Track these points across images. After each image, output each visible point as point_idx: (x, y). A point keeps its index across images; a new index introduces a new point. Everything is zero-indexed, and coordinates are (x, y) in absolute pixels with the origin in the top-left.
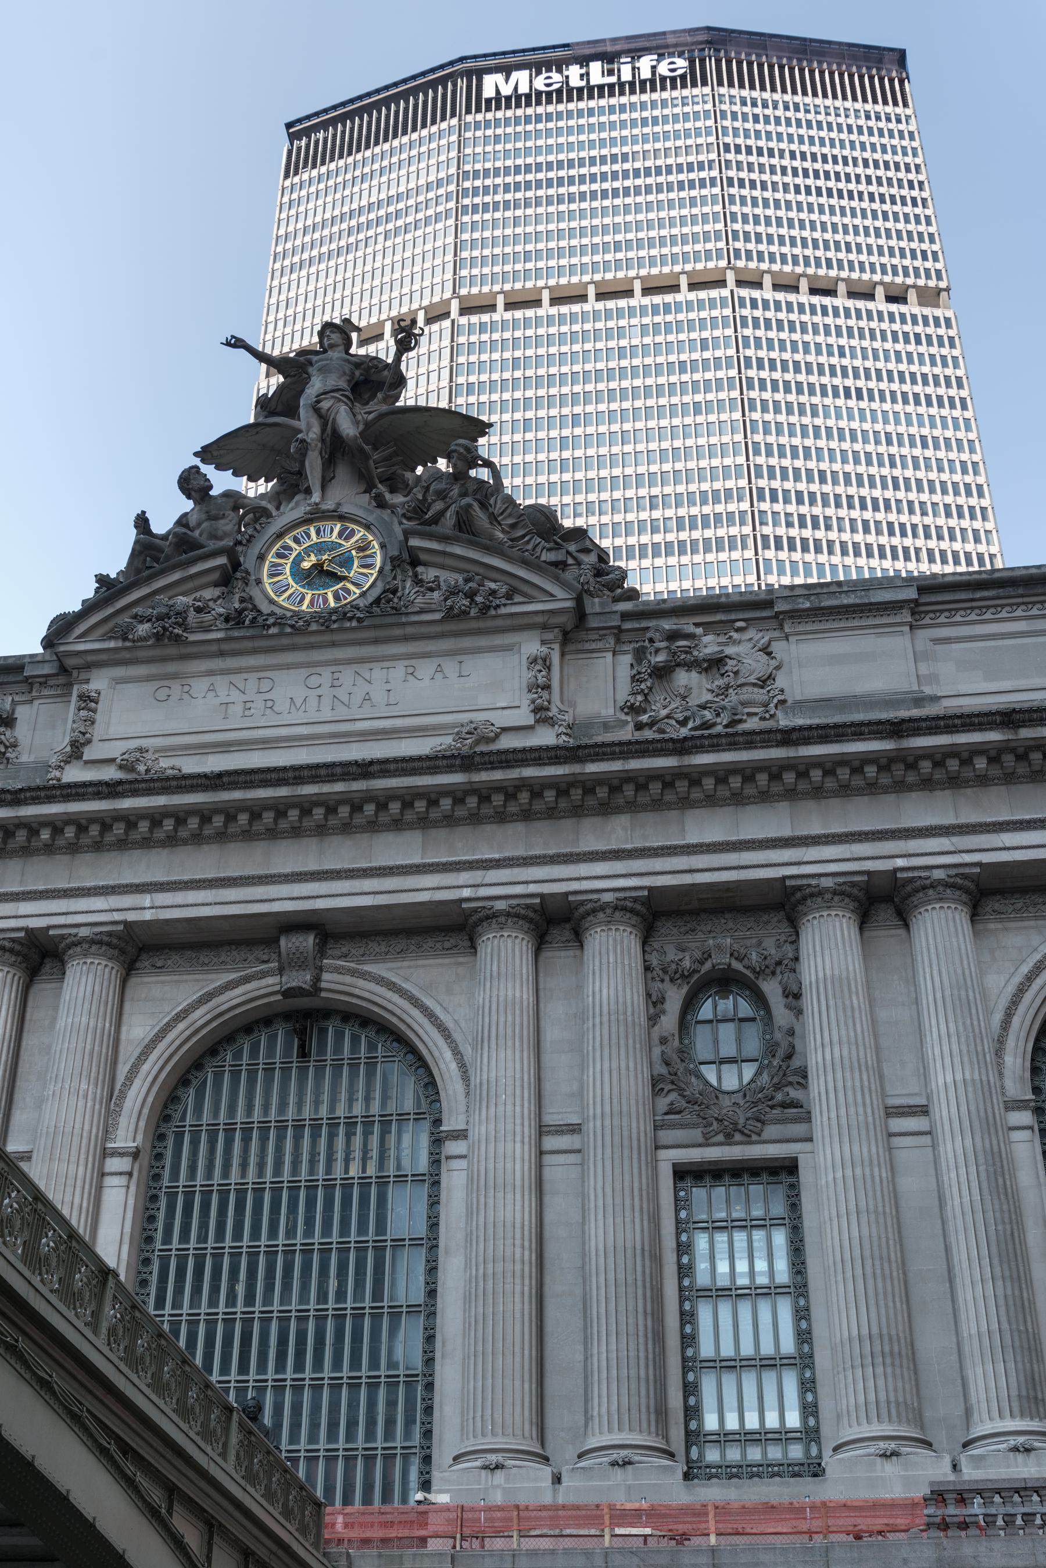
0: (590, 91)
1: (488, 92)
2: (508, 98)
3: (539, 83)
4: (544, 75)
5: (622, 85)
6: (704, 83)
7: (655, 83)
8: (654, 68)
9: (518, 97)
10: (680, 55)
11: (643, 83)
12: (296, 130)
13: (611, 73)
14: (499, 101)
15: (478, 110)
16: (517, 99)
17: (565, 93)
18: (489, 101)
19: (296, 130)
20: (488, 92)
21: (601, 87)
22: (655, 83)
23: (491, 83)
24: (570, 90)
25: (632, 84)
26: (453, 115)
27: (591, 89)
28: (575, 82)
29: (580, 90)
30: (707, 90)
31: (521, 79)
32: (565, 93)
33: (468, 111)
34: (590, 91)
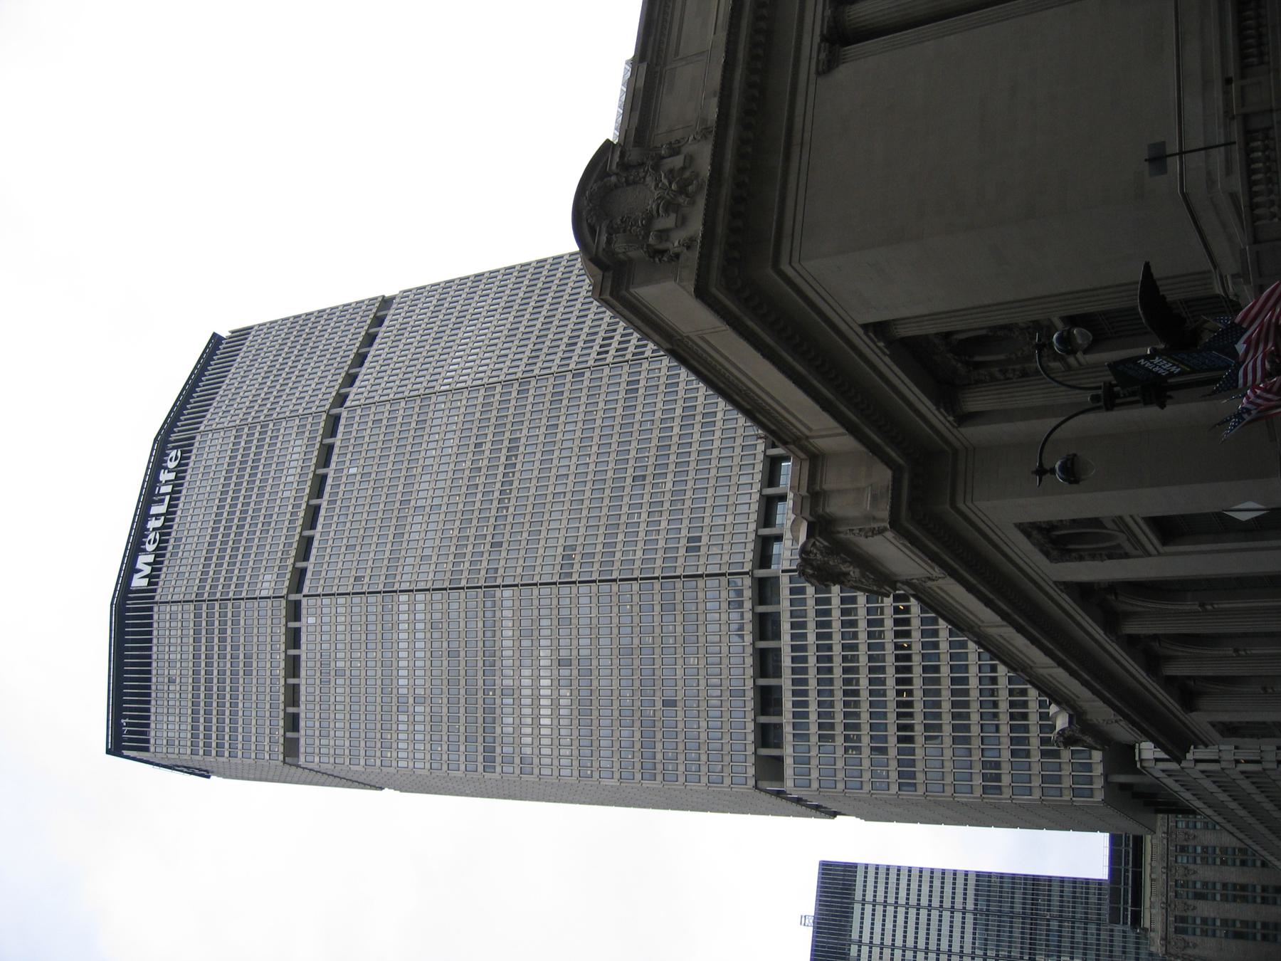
0: (169, 516)
2: (153, 570)
3: (150, 547)
5: (173, 492)
6: (194, 438)
7: (180, 472)
9: (155, 562)
11: (177, 478)
12: (116, 748)
13: (162, 501)
14: (153, 578)
16: (156, 566)
17: (164, 531)
19: (116, 748)
20: (145, 582)
21: (169, 506)
22: (180, 472)
23: (138, 582)
24: (163, 527)
27: (168, 513)
28: (159, 523)
30: (198, 438)
31: (143, 561)
32: (164, 531)
33: (153, 597)
34: (169, 516)
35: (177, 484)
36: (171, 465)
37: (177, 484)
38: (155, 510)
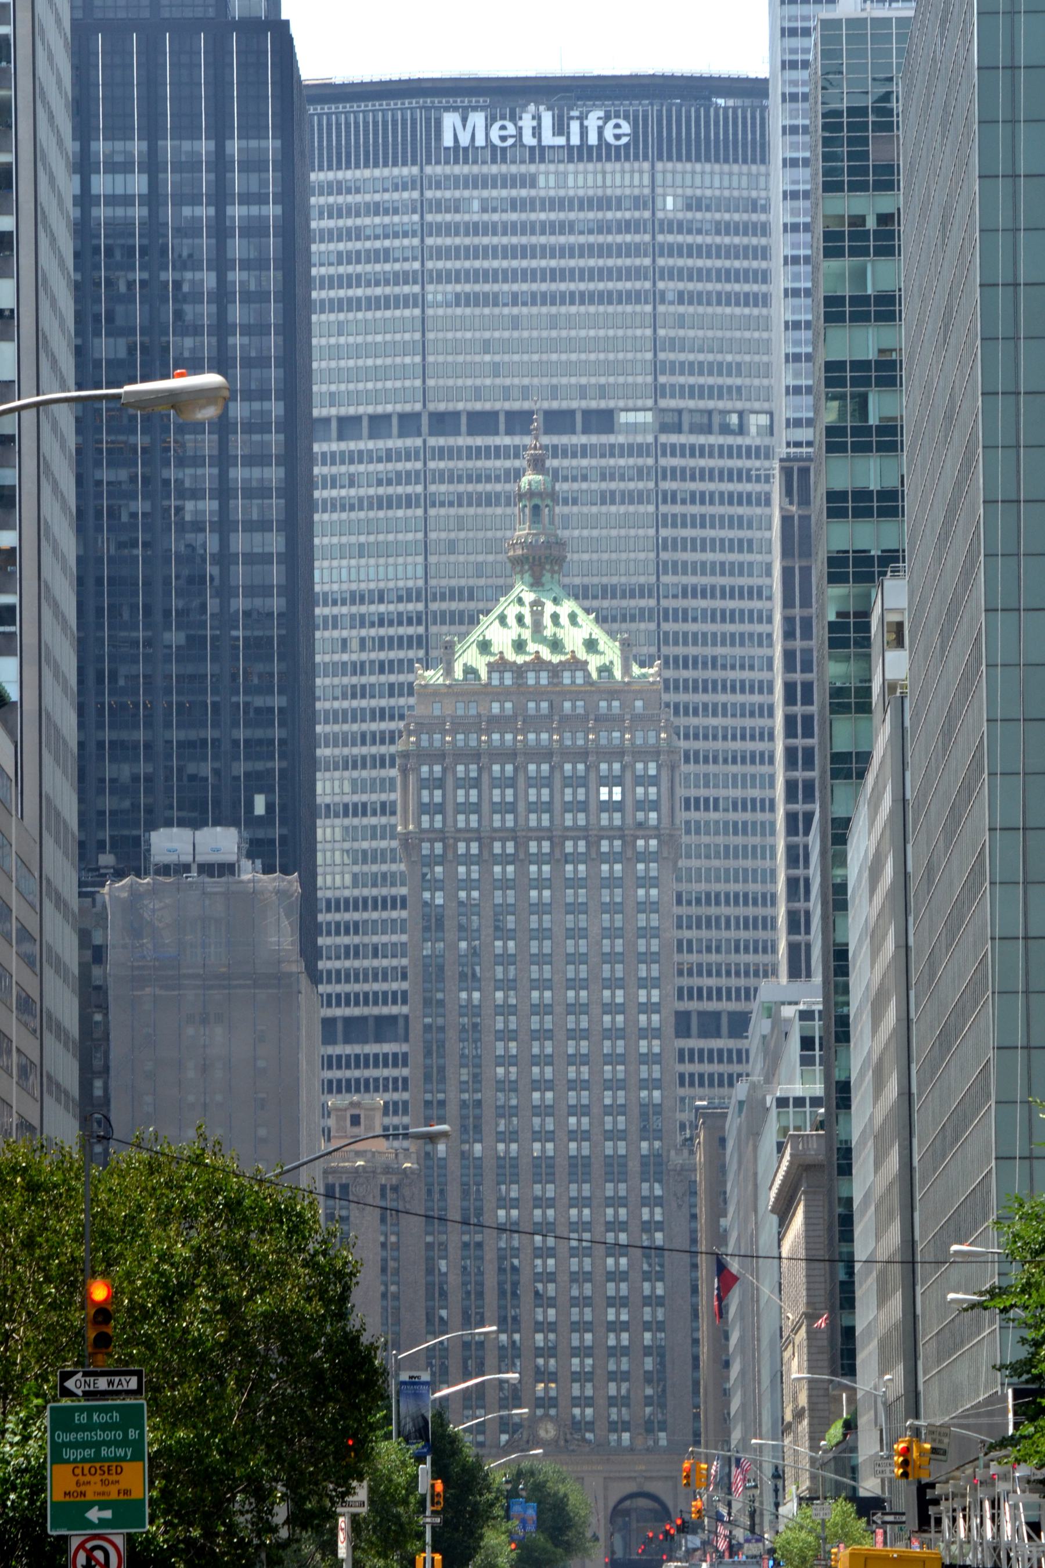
0: (539, 153)
1: (448, 141)
2: (466, 149)
4: (499, 124)
5: (570, 148)
6: (646, 158)
8: (600, 130)
10: (626, 118)
11: (590, 148)
14: (460, 153)
15: (438, 163)
18: (447, 149)
23: (450, 120)
25: (580, 148)
26: (414, 163)
27: (542, 149)
28: (529, 140)
29: (532, 149)
33: (429, 162)
35: (582, 153)
36: (609, 134)
37: (582, 153)
38: (547, 118)
